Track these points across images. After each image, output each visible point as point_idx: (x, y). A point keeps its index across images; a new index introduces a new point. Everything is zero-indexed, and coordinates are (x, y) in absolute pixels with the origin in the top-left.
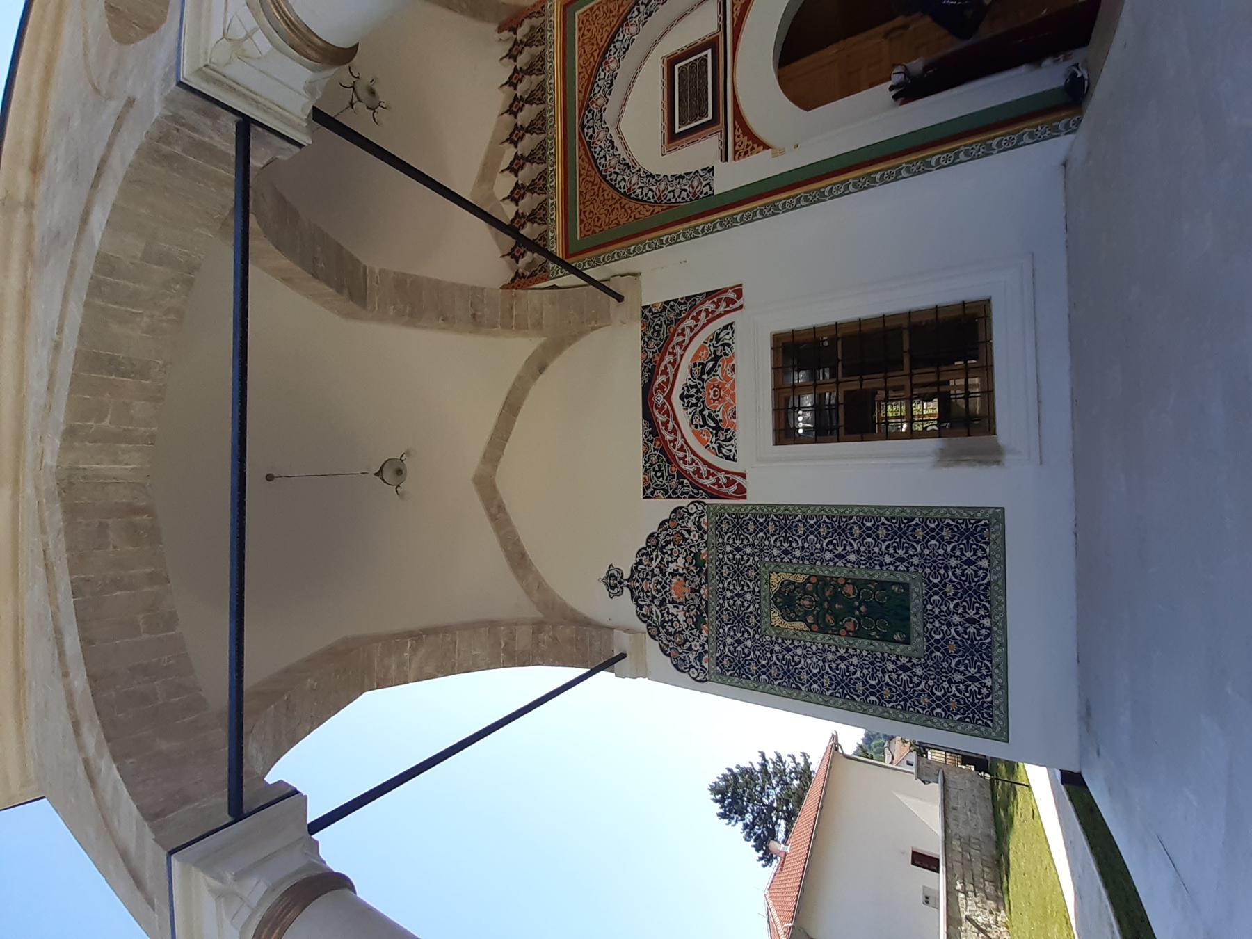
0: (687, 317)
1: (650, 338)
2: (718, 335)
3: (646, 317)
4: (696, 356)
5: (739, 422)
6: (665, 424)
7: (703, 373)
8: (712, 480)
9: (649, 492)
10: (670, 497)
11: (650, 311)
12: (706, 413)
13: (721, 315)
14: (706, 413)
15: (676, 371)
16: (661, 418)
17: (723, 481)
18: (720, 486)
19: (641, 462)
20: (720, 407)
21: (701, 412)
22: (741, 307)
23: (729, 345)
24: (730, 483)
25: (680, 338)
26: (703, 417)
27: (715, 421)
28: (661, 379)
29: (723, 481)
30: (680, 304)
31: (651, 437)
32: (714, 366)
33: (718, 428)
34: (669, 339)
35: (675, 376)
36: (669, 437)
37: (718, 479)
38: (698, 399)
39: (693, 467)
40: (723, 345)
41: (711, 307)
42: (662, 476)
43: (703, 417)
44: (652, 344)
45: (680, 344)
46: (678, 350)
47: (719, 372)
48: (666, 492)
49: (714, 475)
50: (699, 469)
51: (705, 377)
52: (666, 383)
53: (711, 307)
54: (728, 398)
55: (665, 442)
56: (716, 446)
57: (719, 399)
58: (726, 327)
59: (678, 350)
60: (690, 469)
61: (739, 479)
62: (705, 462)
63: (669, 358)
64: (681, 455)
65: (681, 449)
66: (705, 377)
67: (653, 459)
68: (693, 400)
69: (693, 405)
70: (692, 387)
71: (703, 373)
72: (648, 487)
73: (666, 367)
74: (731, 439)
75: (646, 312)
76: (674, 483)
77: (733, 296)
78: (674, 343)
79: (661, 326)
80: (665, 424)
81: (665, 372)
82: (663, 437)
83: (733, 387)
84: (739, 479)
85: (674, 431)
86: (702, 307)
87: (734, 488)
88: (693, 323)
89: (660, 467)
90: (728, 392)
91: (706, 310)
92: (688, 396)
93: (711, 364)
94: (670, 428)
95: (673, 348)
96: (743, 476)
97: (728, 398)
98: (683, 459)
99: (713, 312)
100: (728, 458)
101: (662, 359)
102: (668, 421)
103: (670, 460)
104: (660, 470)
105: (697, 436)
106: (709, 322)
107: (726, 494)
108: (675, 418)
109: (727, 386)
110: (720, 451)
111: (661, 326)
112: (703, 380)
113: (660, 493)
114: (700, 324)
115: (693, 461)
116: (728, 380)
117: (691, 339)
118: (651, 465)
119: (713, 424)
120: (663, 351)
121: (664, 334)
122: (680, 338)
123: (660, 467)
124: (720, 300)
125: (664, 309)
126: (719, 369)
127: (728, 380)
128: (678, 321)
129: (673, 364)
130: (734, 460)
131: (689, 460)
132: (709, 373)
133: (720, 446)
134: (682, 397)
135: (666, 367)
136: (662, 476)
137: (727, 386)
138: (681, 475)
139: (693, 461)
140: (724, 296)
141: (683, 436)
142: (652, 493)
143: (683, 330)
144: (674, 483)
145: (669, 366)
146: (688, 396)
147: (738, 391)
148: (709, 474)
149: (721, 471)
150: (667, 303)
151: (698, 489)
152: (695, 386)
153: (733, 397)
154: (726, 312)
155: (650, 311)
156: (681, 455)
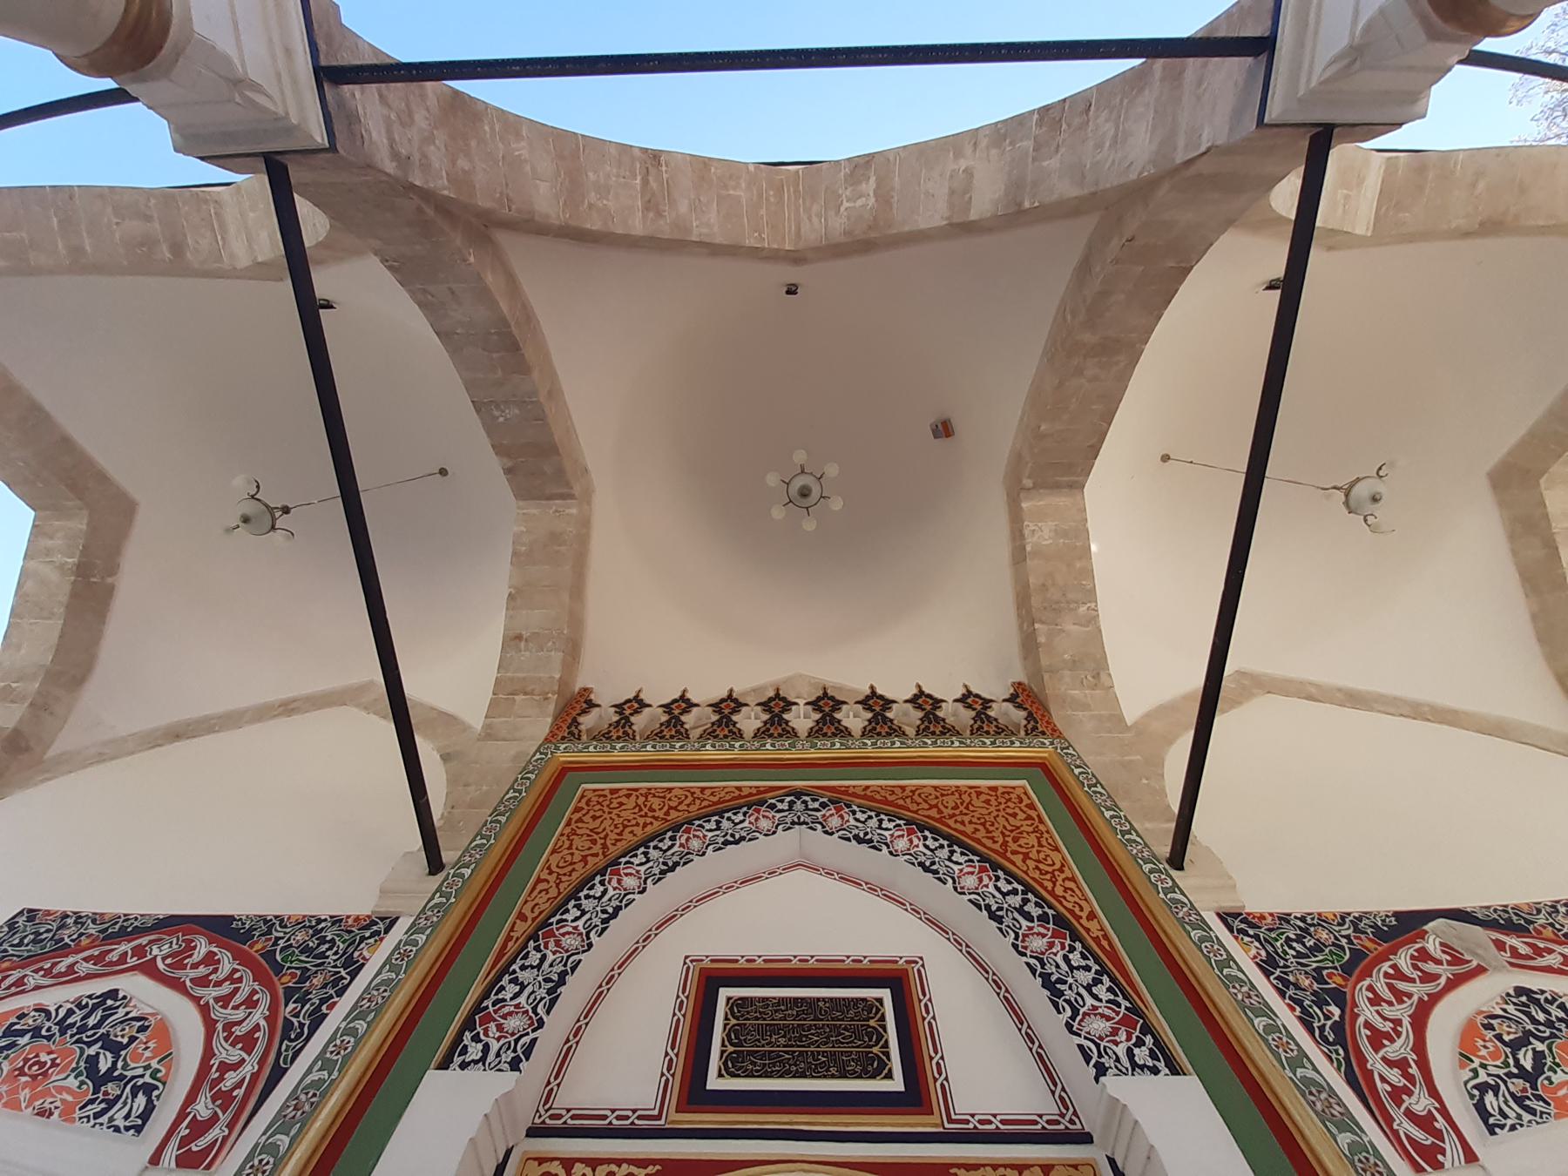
6: (1424, 955)
8: (1394, 1076)
19: (1297, 909)
36: (1403, 960)
37: (1410, 1093)
42: (1299, 955)
60: (1367, 1012)
64: (1386, 994)
85: (1428, 978)
89: (1317, 948)
115: (1397, 1022)
123: (1317, 948)
138: (1339, 997)
139: (1397, 1022)
148: (1402, 1064)
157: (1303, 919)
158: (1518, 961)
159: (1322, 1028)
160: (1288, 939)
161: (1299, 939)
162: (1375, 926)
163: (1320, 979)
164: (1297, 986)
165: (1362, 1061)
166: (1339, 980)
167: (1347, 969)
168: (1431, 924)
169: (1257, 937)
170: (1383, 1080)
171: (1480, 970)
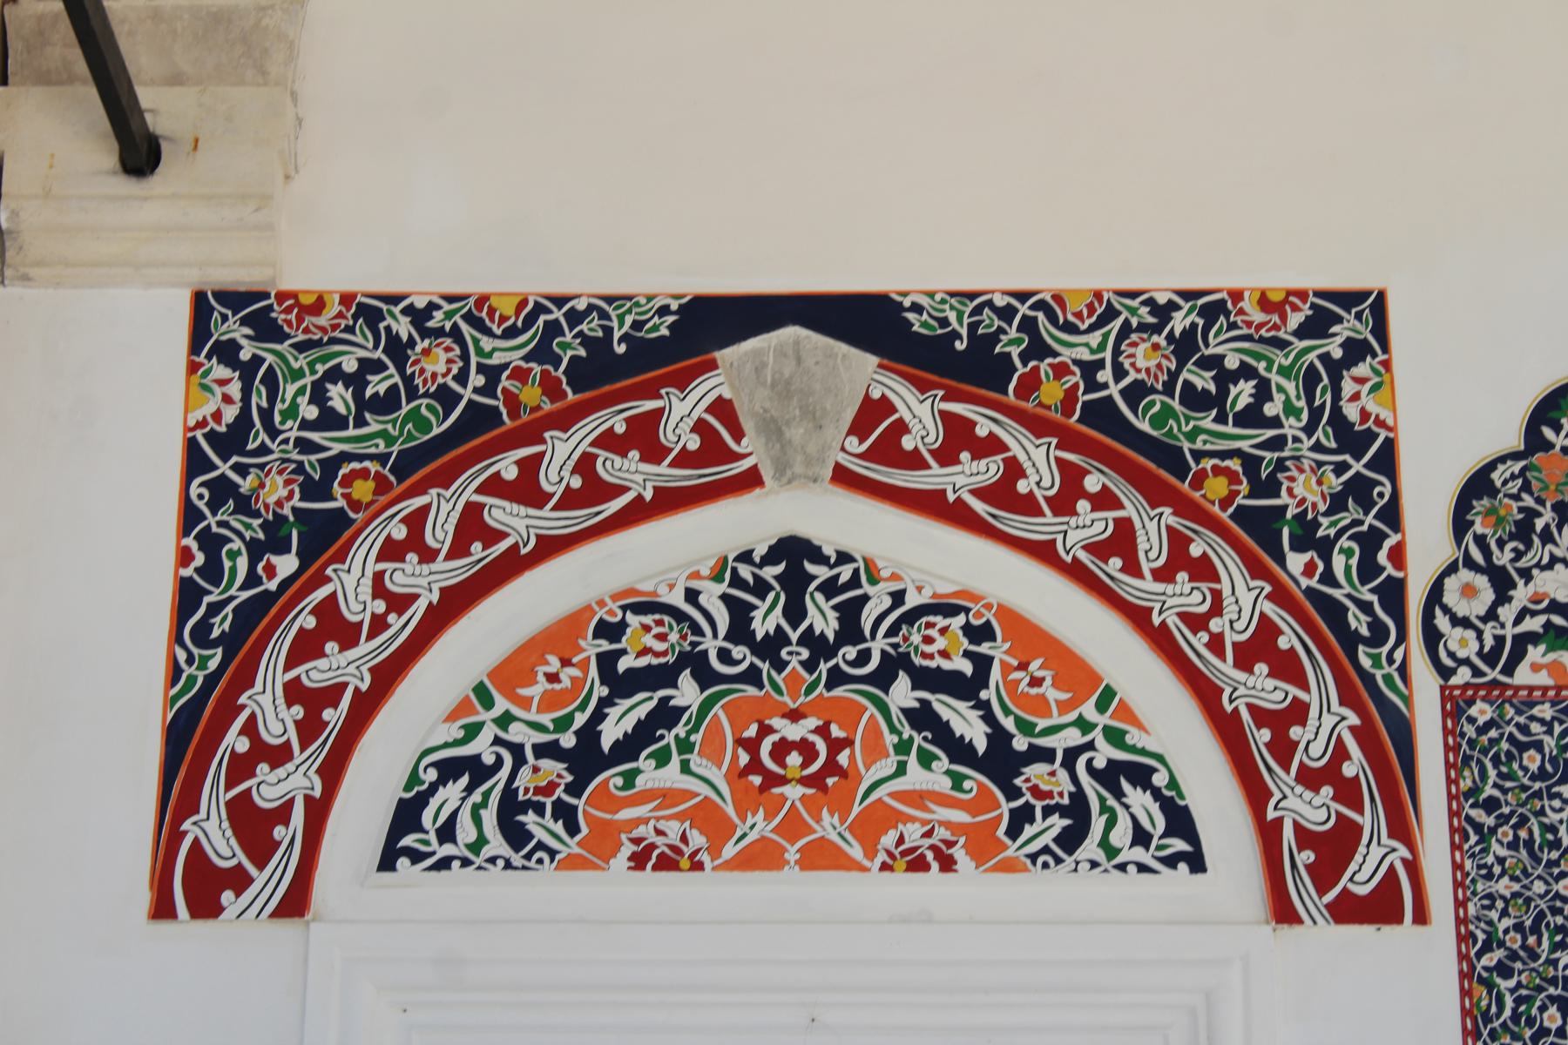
0: (1280, 596)
1: (1185, 346)
2: (1141, 776)
3: (1317, 326)
4: (1033, 640)
5: (618, 884)
6: (643, 438)
7: (925, 679)
8: (279, 722)
9: (232, 329)
10: (195, 462)
11: (1356, 351)
12: (687, 692)
13: (1256, 794)
14: (687, 692)
15: (956, 515)
16: (681, 414)
17: (269, 787)
18: (241, 768)
19: (422, 287)
20: (711, 776)
21: (696, 663)
22: (1284, 912)
23: (1071, 840)
24: (255, 827)
25: (1151, 545)
26: (663, 676)
27: (628, 748)
28: (920, 414)
29: (269, 787)
30: (1371, 542)
31: (570, 348)
32: (959, 750)
33: (586, 759)
34: (1161, 469)
35: (932, 505)
36: (560, 454)
37: (279, 756)
38: (771, 647)
39: (358, 605)
40: (1077, 809)
41: (1313, 743)
42: (330, 420)
43: (663, 676)
44: (1144, 358)
45: (1122, 542)
46: (1083, 529)
47: (916, 777)
48: (232, 440)
49: (309, 729)
50: (348, 635)
51: (902, 693)
52: (889, 451)
53: (1313, 743)
54: (759, 826)
55: (531, 433)
56: (482, 747)
57: (758, 780)
58: (1180, 821)
59: (1083, 529)
61: (271, 881)
62: (388, 675)
63: (1040, 464)
65: (472, 526)
66: (902, 693)
67: (437, 363)
68: (765, 622)
69: (740, 614)
70: (850, 613)
71: (925, 679)
72: (266, 329)
73: (992, 446)
74: (516, 836)
75: (1349, 327)
76: (276, 491)
77: (1361, 876)
78: (1133, 506)
79: (1252, 417)
80: (643, 438)
81: (958, 439)
82: (565, 420)
83: (822, 857)
84: (271, 881)
85: (594, 490)
86: (1321, 689)
87: (223, 847)
88: (1235, 626)
89: (386, 403)
90: (792, 827)
91: (1298, 712)
92: (795, 583)
93: (974, 731)
94: (611, 467)
95: (1104, 501)
96: (295, 904)
97: (759, 826)
98: (415, 544)
99: (1283, 750)
100: (407, 815)
101: (1037, 426)
102: (653, 453)
103: (420, 466)
104: (365, 406)
105: (558, 638)
106: (1228, 730)
107: (189, 805)
108: (669, 501)
109: (829, 826)
110: (449, 770)
111: (1252, 417)
112: (883, 678)
113: (221, 400)
114: (1224, 670)
115: (400, 603)
116: (869, 828)
117: (1138, 617)
118: (398, 350)
119: (611, 732)
120: (1100, 428)
121: (1202, 433)
122: (1151, 545)
123: (386, 403)
124: (1348, 793)
125: (1351, 439)
126: (937, 779)
127: (869, 828)
128: (1260, 532)
129: (1003, 493)
130: (387, 863)
131: (407, 575)
132: (922, 717)
133: (478, 771)
134: (794, 552)
135: (992, 446)
136: (330, 420)
137: (829, 826)
138: (325, 537)
140: (1371, 818)
141: (549, 547)
142: (227, 352)
143: (1203, 570)
144: (276, 491)
145: (989, 470)
146: (795, 583)
147: (790, 886)
149: (332, 772)
150: (1387, 461)
151: (230, 643)
152: (850, 630)
153: (761, 857)
154: (1269, 834)
155: (1356, 351)
156: (440, 532)
157: (419, 317)
158: (878, 459)
159: (215, 609)
160: (335, 374)
161: (356, 381)
162: (598, 346)
163: (315, 489)
164: (245, 506)
165: (245, 679)
166: (363, 490)
167: (406, 464)
168: (728, 352)
169: (248, 371)
170: (250, 729)
171: (751, 480)
